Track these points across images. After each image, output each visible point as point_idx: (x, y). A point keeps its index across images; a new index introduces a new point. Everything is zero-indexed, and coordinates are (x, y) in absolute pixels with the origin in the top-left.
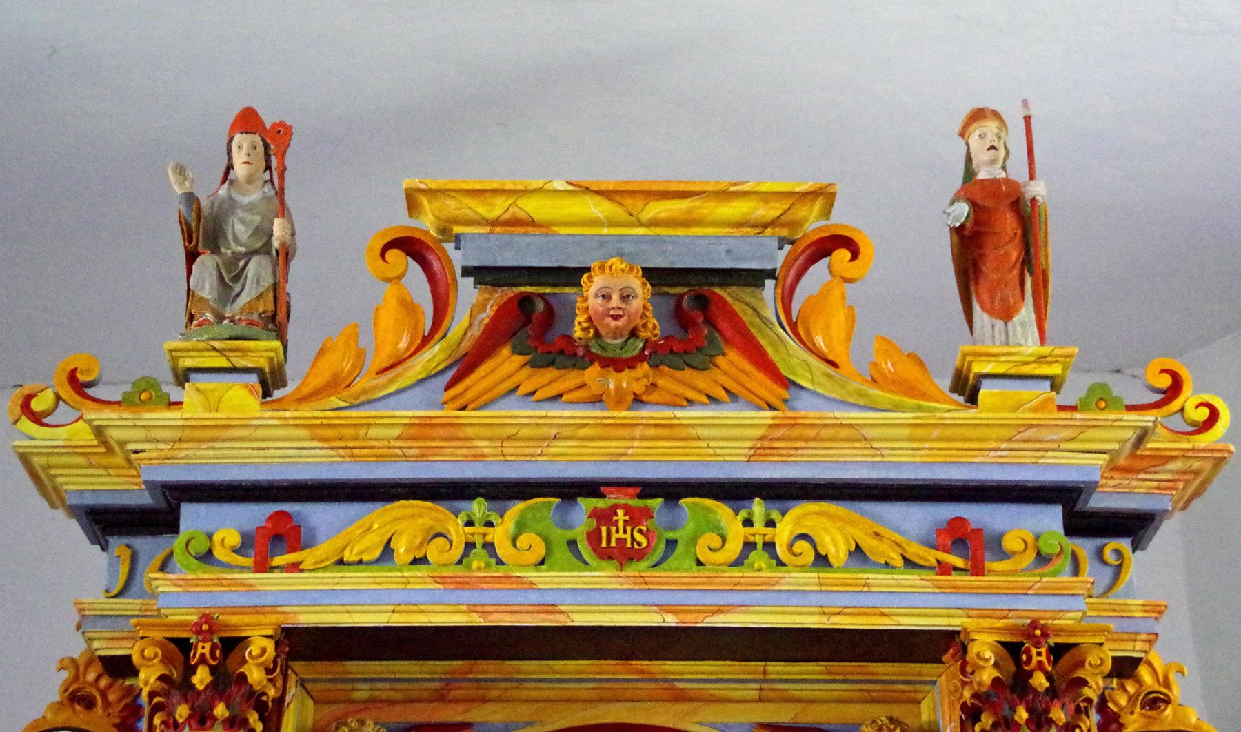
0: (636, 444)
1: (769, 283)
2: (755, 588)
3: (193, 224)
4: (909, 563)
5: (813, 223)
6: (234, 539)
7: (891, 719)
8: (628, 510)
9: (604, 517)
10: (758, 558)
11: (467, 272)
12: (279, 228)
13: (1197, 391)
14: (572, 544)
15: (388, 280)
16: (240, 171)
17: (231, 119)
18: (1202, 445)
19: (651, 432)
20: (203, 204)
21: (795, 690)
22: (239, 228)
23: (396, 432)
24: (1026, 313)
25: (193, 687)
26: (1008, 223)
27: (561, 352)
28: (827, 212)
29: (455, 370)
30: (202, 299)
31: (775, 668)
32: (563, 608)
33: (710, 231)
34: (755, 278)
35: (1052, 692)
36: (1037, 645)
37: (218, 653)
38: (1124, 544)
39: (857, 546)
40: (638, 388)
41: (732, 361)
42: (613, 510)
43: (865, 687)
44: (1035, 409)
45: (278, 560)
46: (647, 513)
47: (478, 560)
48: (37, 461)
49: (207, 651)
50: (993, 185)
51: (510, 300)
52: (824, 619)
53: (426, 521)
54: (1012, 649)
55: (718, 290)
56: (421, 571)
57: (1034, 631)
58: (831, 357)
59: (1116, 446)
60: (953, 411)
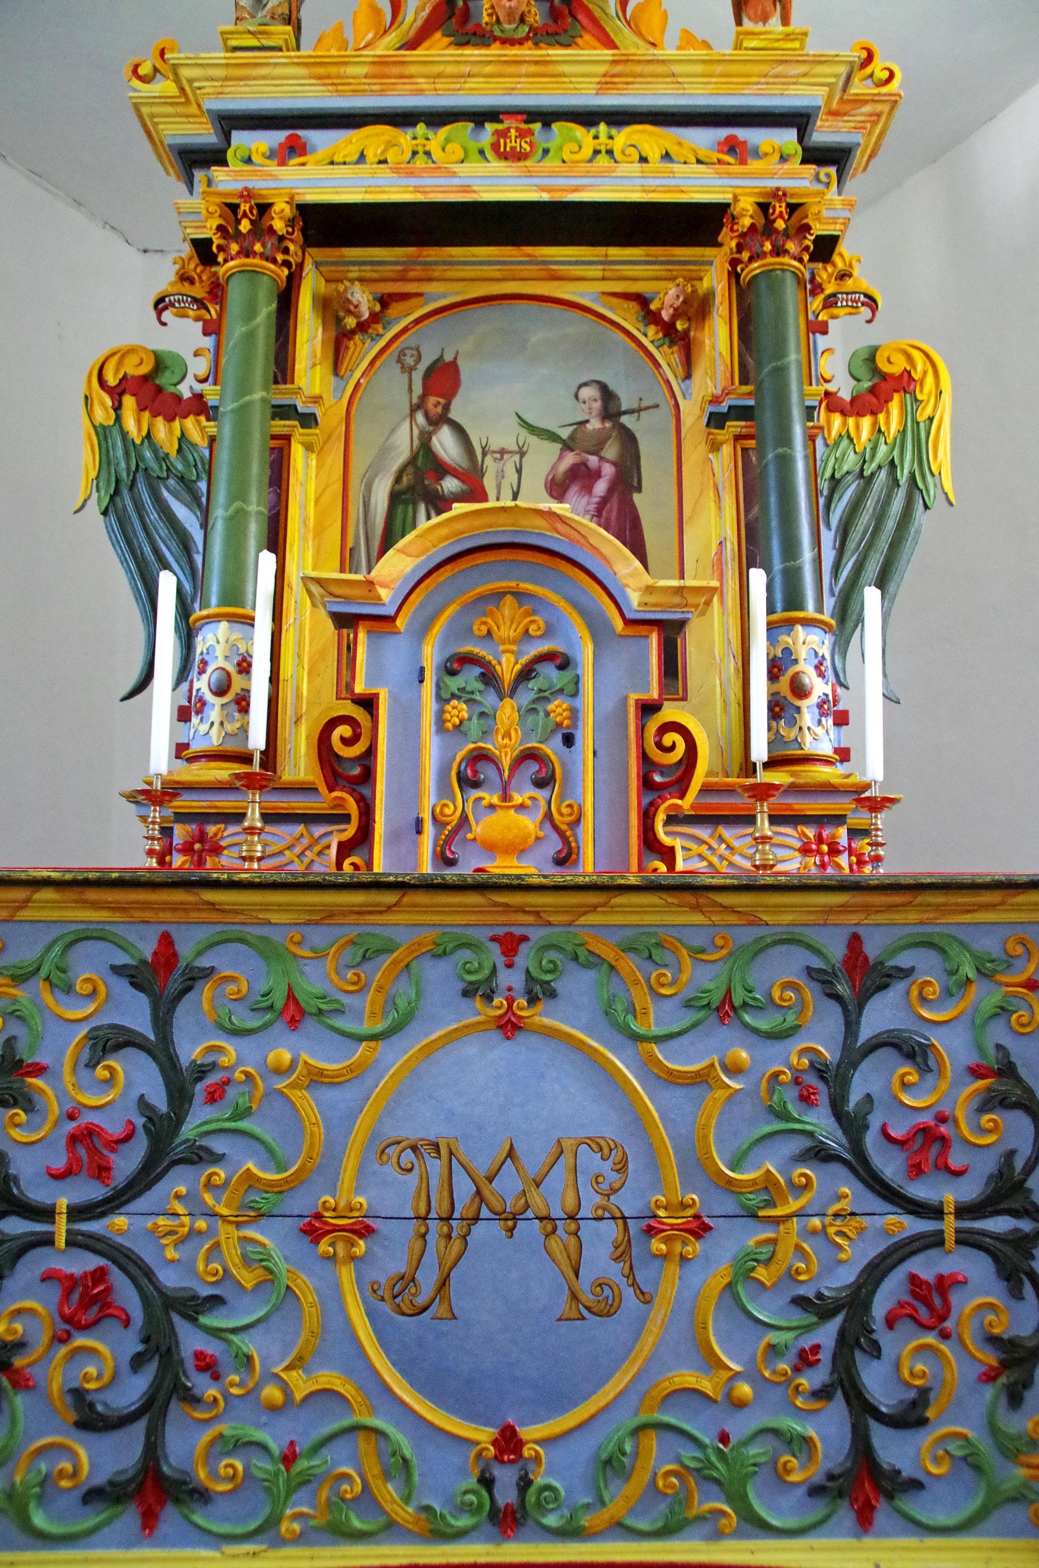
0: (522, 80)
2: (601, 174)
4: (699, 162)
8: (517, 129)
9: (504, 134)
14: (482, 152)
25: (240, 231)
27: (475, 34)
32: (475, 188)
36: (780, 201)
37: (255, 212)
46: (531, 133)
47: (420, 162)
52: (644, 195)
53: (387, 138)
54: (764, 208)
57: (777, 194)
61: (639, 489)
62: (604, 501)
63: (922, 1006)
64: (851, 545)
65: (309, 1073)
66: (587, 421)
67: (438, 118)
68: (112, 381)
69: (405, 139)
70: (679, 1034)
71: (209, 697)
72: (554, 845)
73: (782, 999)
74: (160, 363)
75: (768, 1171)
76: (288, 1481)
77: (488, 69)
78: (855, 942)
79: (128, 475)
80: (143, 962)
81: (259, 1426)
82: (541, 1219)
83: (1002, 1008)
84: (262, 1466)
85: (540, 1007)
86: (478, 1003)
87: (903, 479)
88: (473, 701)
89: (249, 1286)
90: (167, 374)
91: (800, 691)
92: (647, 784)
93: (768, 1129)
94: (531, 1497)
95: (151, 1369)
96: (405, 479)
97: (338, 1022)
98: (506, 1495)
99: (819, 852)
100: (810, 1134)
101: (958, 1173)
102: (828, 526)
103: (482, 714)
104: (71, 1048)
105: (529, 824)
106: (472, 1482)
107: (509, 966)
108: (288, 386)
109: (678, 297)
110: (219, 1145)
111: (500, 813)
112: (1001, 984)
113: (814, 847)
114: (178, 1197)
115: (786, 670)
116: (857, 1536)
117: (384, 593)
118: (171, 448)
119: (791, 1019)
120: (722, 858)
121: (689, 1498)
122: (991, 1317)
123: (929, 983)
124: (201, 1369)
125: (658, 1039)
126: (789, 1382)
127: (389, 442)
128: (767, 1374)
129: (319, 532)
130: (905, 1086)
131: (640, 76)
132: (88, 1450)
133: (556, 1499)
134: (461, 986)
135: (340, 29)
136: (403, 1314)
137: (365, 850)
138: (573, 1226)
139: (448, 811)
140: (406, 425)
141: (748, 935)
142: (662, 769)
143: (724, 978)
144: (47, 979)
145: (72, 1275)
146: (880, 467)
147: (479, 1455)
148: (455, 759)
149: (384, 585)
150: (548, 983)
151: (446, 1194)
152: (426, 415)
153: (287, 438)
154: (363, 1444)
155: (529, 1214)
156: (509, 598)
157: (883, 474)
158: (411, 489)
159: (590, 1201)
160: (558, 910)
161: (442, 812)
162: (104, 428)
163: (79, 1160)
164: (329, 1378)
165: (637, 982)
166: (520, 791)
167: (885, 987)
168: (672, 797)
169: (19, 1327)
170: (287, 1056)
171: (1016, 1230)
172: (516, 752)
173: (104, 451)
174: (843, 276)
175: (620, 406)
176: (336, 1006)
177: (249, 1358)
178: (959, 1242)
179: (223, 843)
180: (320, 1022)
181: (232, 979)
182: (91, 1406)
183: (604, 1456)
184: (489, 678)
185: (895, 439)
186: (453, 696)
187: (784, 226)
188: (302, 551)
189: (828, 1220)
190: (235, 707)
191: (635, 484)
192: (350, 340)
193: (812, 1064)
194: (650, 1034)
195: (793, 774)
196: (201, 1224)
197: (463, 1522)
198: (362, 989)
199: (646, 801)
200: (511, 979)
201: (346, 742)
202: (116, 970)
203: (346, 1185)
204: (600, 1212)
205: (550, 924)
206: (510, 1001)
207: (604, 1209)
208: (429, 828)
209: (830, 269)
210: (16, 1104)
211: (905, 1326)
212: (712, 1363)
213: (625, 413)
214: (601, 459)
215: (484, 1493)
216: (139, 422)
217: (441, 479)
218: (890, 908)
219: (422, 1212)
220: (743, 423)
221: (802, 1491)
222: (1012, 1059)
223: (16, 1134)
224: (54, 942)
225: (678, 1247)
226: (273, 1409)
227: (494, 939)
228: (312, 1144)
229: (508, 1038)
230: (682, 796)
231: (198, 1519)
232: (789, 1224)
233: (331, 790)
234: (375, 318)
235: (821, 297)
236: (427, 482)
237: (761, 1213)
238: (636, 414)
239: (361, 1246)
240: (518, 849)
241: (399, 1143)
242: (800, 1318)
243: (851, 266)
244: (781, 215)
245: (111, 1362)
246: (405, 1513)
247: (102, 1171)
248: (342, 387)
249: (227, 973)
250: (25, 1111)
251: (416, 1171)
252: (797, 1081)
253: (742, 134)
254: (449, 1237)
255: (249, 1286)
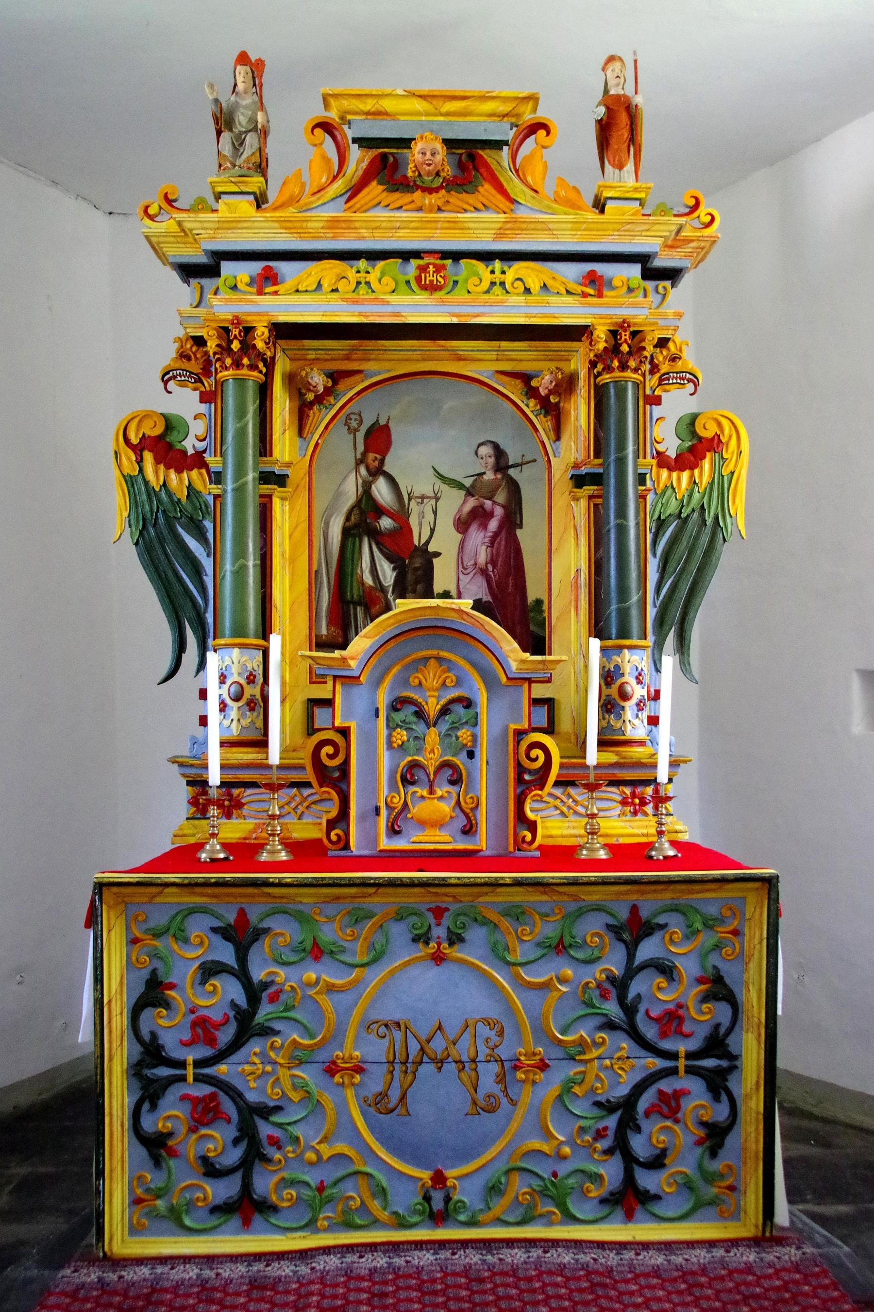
1: (505, 148)
3: (219, 116)
4: (568, 292)
5: (528, 117)
6: (247, 279)
7: (557, 368)
8: (435, 265)
10: (497, 289)
11: (355, 140)
12: (260, 117)
13: (708, 206)
15: (315, 145)
16: (241, 87)
17: (235, 58)
18: (706, 234)
19: (446, 225)
20: (223, 105)
21: (514, 355)
22: (241, 117)
23: (321, 225)
24: (630, 166)
26: (623, 118)
27: (402, 184)
28: (535, 110)
29: (349, 194)
30: (225, 156)
31: (504, 344)
32: (404, 314)
33: (475, 119)
34: (498, 145)
35: (630, 353)
36: (625, 331)
38: (668, 284)
39: (545, 284)
40: (440, 203)
41: (486, 189)
42: (428, 264)
43: (546, 353)
44: (633, 215)
45: (268, 289)
46: (444, 267)
48: (154, 240)
49: (237, 333)
50: (618, 97)
51: (375, 157)
52: (527, 319)
54: (614, 333)
55: (480, 152)
56: (335, 295)
57: (624, 324)
58: (535, 188)
59: (667, 234)
60: (592, 216)
61: (521, 527)
62: (496, 535)
63: (671, 945)
64: (670, 569)
65: (327, 985)
66: (484, 473)
67: (374, 256)
68: (135, 440)
69: (350, 271)
70: (533, 961)
71: (228, 701)
72: (462, 821)
73: (591, 942)
74: (170, 424)
75: (582, 1036)
76: (321, 1201)
77: (412, 225)
78: (634, 909)
79: (152, 515)
80: (230, 925)
81: (304, 1173)
82: (456, 1062)
83: (716, 946)
84: (307, 1193)
85: (456, 947)
86: (421, 945)
87: (709, 521)
88: (412, 729)
89: (296, 1100)
90: (175, 433)
91: (625, 696)
92: (519, 780)
93: (582, 1013)
94: (451, 1206)
95: (244, 1145)
96: (353, 518)
97: (342, 957)
98: (438, 1204)
99: (633, 804)
100: (606, 1015)
101: (688, 1036)
102: (654, 555)
103: (416, 738)
104: (191, 972)
105: (446, 808)
106: (419, 1199)
107: (438, 925)
108: (268, 458)
109: (551, 382)
110: (277, 1026)
111: (428, 802)
112: (717, 932)
113: (630, 800)
114: (255, 1054)
115: (616, 680)
116: (626, 1223)
117: (353, 664)
118: (182, 495)
119: (596, 953)
120: (569, 808)
121: (535, 1206)
122: (702, 1112)
123: (677, 932)
124: (271, 1144)
125: (521, 965)
126: (591, 1146)
127: (342, 488)
128: (579, 1142)
129: (293, 561)
130: (659, 989)
131: (525, 229)
132: (211, 1187)
133: (465, 1207)
134: (411, 936)
135: (299, 174)
136: (381, 1113)
137: (344, 825)
138: (474, 1066)
139: (395, 800)
140: (353, 476)
141: (573, 907)
142: (530, 772)
143: (559, 931)
144: (174, 936)
145: (197, 1097)
146: (693, 510)
147: (423, 1185)
148: (399, 766)
149: (353, 658)
150: (460, 934)
151: (404, 1050)
152: (368, 468)
153: (270, 497)
154: (361, 1181)
155: (450, 1059)
156: (432, 661)
157: (696, 515)
158: (356, 526)
159: (483, 1052)
160: (465, 895)
161: (391, 801)
162: (131, 477)
163: (198, 1036)
164: (342, 1147)
165: (510, 933)
166: (440, 787)
167: (650, 934)
168: (536, 789)
169: (169, 1125)
170: (314, 976)
171: (720, 1066)
172: (438, 763)
173: (132, 495)
174: (674, 359)
175: (507, 462)
176: (342, 949)
177: (297, 1139)
178: (686, 1072)
179: (243, 801)
180: (334, 958)
181: (282, 934)
182: (212, 1165)
183: (490, 1185)
184: (420, 714)
185: (706, 489)
186: (398, 726)
187: (628, 349)
188: (282, 577)
189: (614, 1061)
190: (247, 708)
191: (518, 522)
192: (311, 409)
193: (607, 977)
194: (517, 962)
195: (617, 754)
196: (269, 1068)
197: (415, 1219)
198: (356, 939)
199: (519, 791)
200: (439, 932)
201: (331, 757)
202: (214, 930)
203: (349, 1046)
204: (489, 1058)
205: (461, 901)
206: (439, 944)
207: (491, 1056)
208: (384, 812)
209: (665, 352)
210: (160, 1005)
211: (654, 1117)
212: (548, 1135)
213: (512, 466)
214: (494, 502)
215: (427, 1205)
216: (156, 473)
217: (379, 518)
218: (655, 891)
219: (391, 1059)
220: (595, 487)
221: (596, 1201)
222: (722, 974)
223: (162, 1022)
224: (177, 914)
225: (531, 1076)
226: (311, 1164)
227: (429, 910)
228: (329, 1025)
229: (438, 965)
230: (542, 789)
231: (273, 1220)
232: (593, 1063)
233: (321, 786)
234: (328, 391)
235: (658, 375)
236: (368, 521)
237: (577, 1058)
238: (519, 468)
239: (358, 1078)
240: (439, 824)
241: (377, 1022)
242: (596, 1112)
243: (681, 350)
244: (626, 341)
245: (221, 1142)
246: (384, 1215)
247: (211, 1041)
248: (305, 447)
249: (278, 931)
250: (166, 1009)
251: (387, 1038)
252: (599, 986)
253: (601, 268)
254: (406, 1072)
255: (296, 1100)
